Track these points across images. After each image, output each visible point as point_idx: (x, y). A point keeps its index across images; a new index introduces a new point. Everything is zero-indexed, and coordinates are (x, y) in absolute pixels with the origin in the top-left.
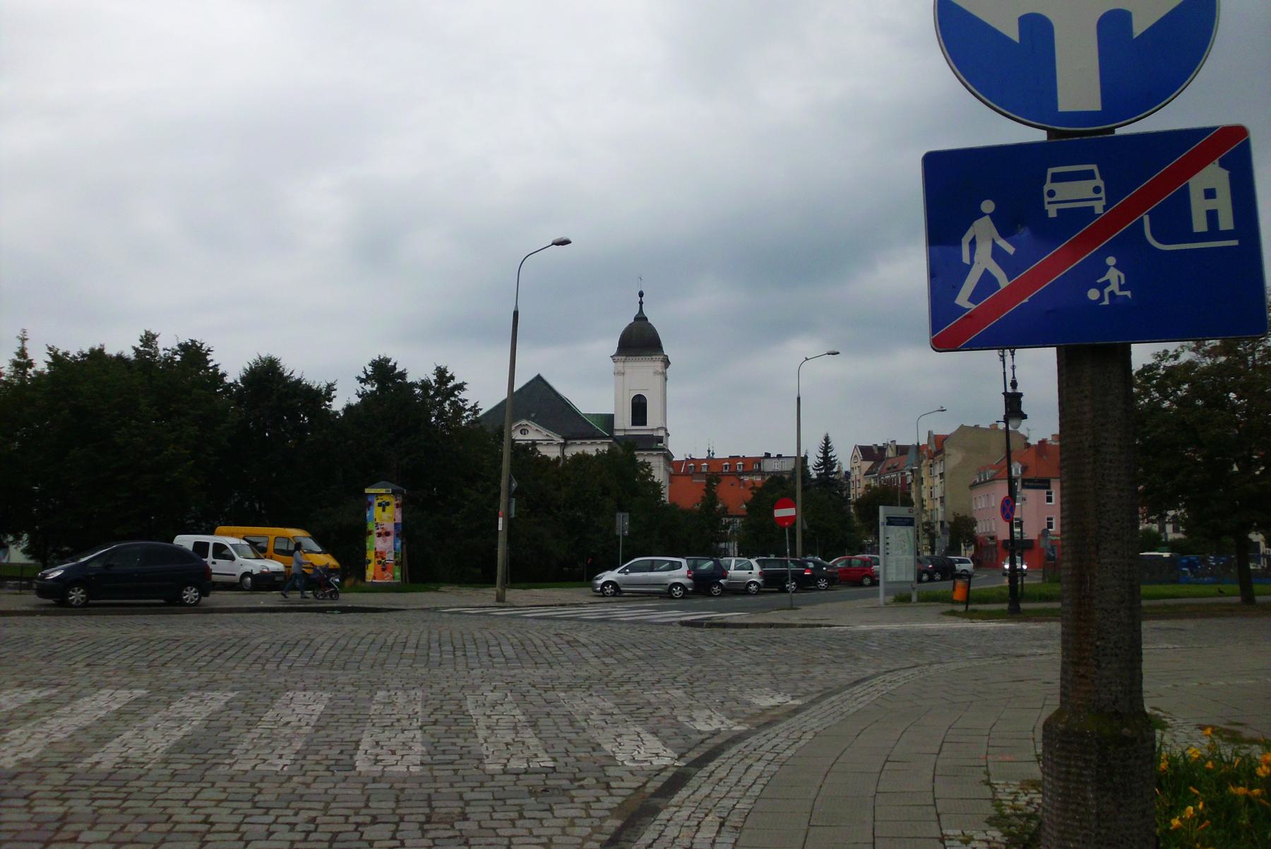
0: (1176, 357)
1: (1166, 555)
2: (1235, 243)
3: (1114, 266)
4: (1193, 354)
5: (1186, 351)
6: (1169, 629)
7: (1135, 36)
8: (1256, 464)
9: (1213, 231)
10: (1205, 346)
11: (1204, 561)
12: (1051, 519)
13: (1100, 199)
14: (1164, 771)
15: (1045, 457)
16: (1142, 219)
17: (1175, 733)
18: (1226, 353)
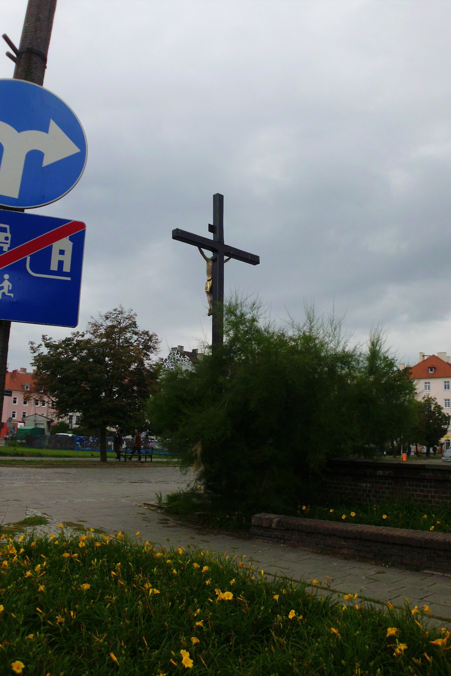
0: (83, 336)
1: (70, 435)
2: (69, 279)
3: (8, 280)
4: (92, 335)
5: (89, 333)
6: (63, 473)
7: (43, 166)
8: (114, 393)
9: (60, 272)
10: (97, 332)
11: (88, 439)
12: (14, 412)
13: (7, 243)
14: (34, 546)
15: (15, 379)
16: (26, 258)
17: (51, 526)
18: (107, 338)
